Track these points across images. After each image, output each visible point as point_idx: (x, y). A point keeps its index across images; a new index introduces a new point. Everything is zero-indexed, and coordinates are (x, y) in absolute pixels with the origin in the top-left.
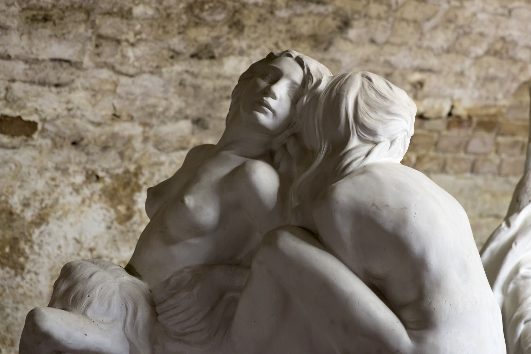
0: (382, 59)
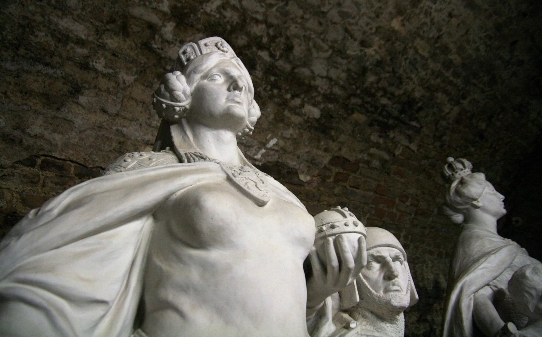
0: (114, 128)
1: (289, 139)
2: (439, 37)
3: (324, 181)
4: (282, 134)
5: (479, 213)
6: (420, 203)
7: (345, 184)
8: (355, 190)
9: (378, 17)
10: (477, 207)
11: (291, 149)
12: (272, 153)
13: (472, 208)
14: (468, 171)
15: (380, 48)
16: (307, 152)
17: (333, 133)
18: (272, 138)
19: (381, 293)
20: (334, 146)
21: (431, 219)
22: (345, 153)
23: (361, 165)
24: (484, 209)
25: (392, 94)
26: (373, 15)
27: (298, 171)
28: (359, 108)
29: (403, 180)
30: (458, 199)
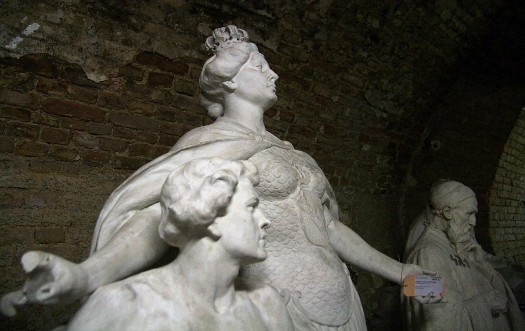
1: (58, 25)
3: (130, 83)
4: (46, 17)
5: (233, 100)
6: (296, 118)
7: (168, 89)
8: (186, 96)
10: (231, 91)
11: (67, 38)
12: (34, 42)
13: (226, 92)
16: (94, 44)
17: (134, 21)
18: (29, 22)
20: (137, 37)
22: (157, 46)
23: (191, 65)
24: (241, 94)
27: (85, 69)
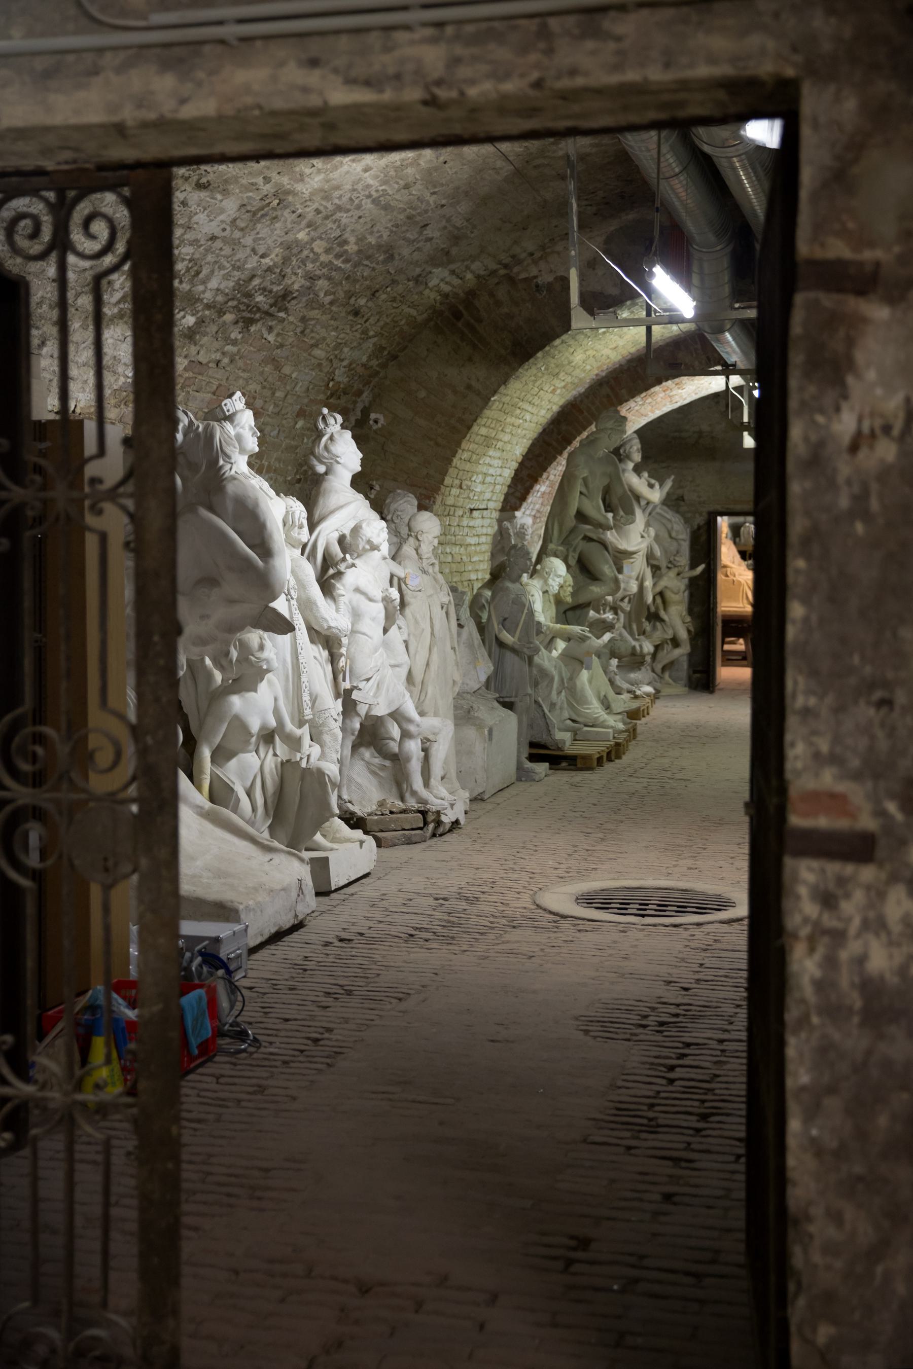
2: (340, 236)
5: (338, 468)
9: (286, 234)
10: (338, 463)
14: (338, 427)
15: (277, 255)
19: (296, 535)
21: (262, 420)
24: (345, 466)
25: (271, 292)
26: (284, 234)
28: (232, 310)
29: (245, 375)
30: (326, 454)
